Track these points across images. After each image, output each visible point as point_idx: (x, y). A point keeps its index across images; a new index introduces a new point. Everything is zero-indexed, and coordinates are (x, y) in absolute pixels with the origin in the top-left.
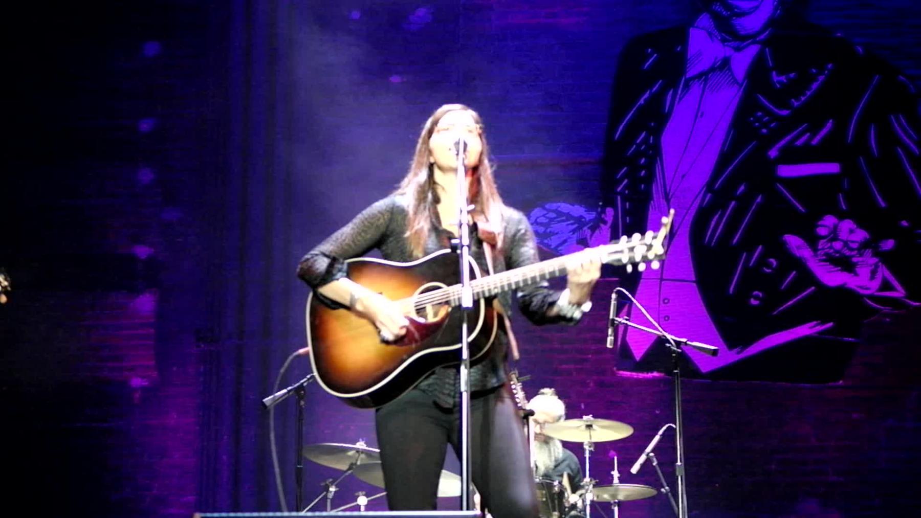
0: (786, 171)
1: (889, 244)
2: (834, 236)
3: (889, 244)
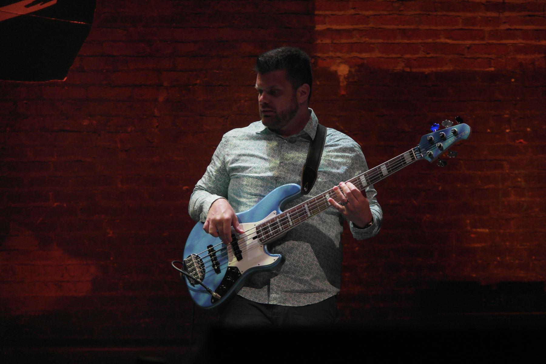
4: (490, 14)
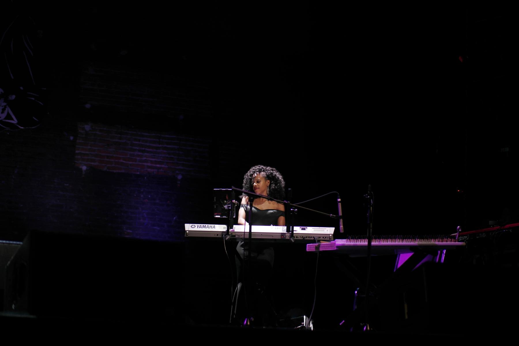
1: (14, 97)
3: (14, 97)
4: (140, 153)
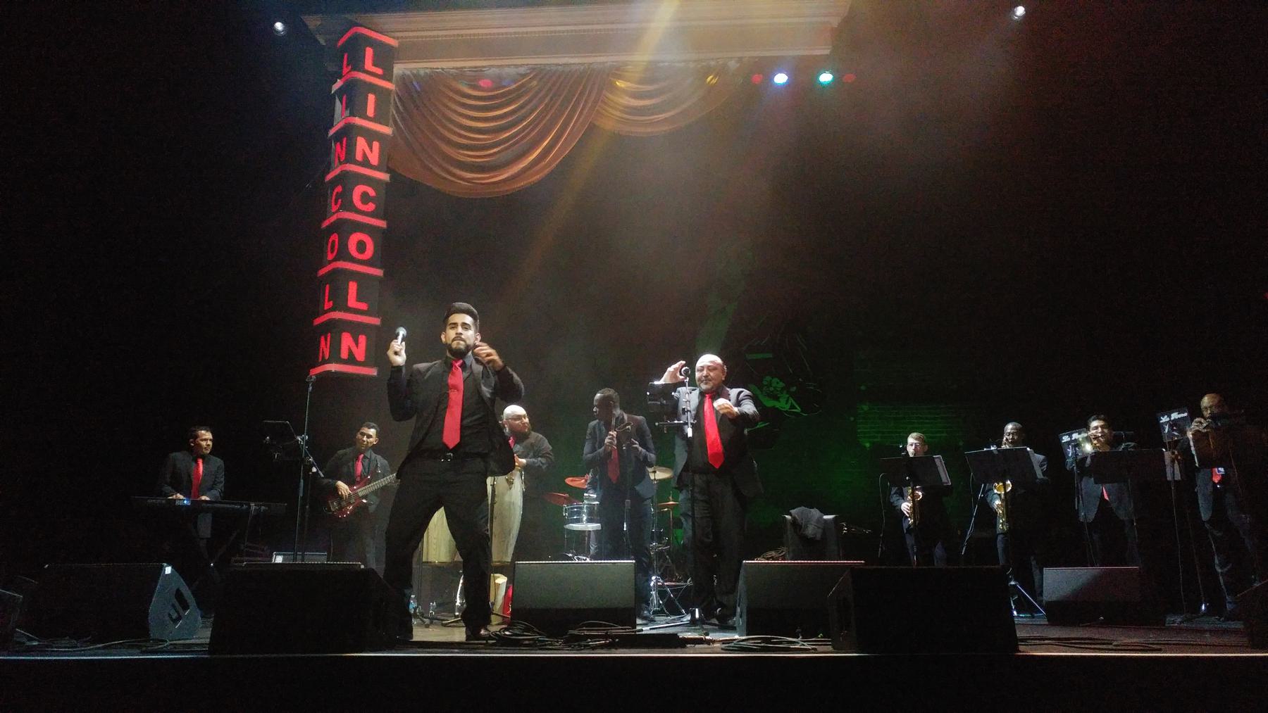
0: (750, 357)
1: (794, 389)
2: (770, 384)
3: (794, 389)
